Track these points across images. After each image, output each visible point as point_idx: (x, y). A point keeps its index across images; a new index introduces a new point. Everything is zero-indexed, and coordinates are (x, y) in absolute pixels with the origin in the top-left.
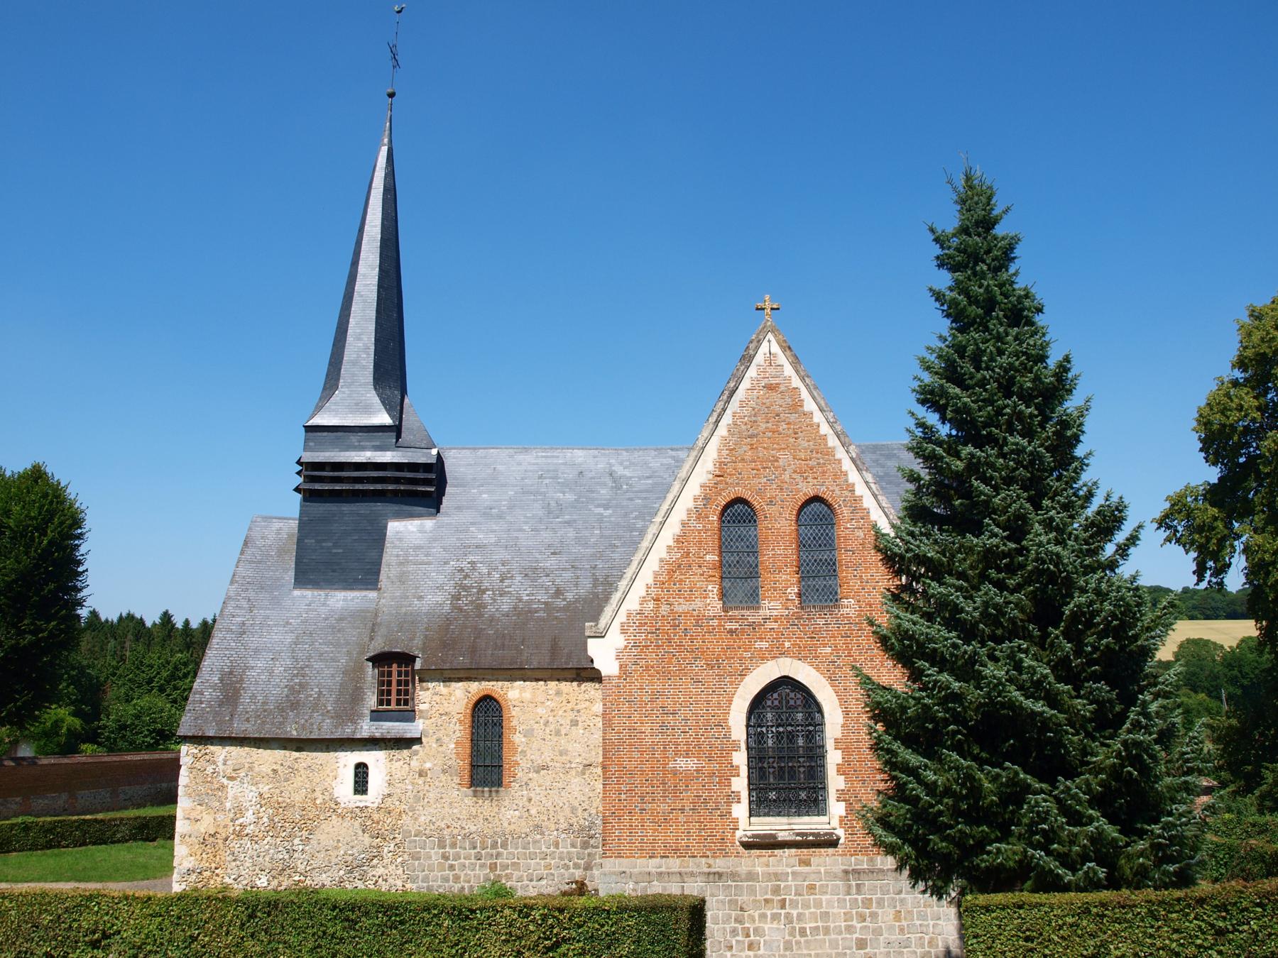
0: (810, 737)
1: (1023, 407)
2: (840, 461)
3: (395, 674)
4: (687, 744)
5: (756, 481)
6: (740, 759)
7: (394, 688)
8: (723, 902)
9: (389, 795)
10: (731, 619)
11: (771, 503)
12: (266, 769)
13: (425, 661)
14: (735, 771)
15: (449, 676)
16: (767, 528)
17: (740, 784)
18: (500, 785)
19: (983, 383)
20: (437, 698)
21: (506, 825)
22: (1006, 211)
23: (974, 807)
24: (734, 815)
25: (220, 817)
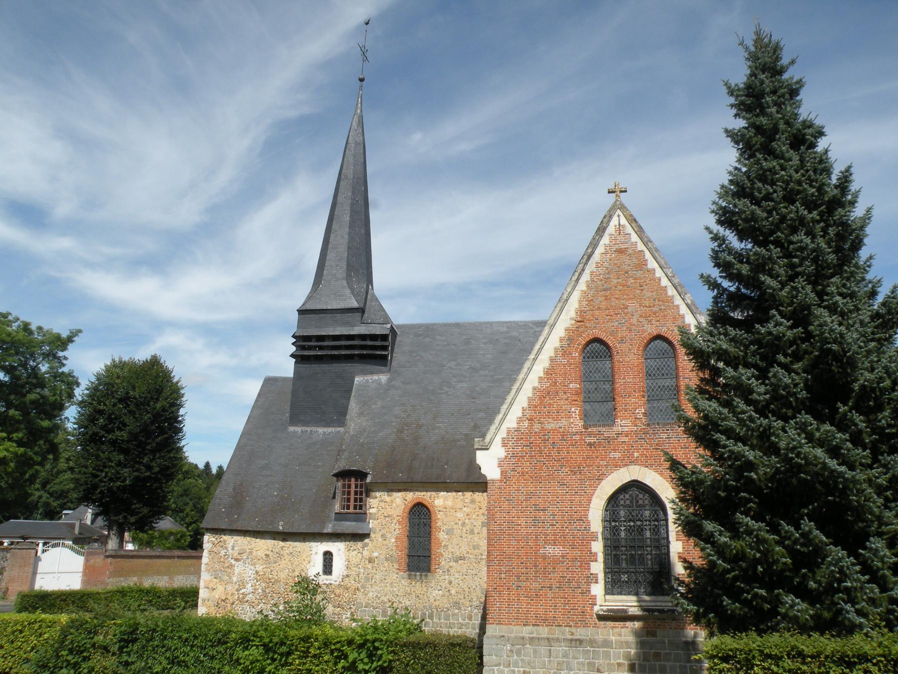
0: (656, 530)
1: (806, 212)
2: (678, 307)
3: (353, 486)
4: (555, 535)
5: (610, 324)
6: (598, 547)
7: (352, 497)
8: (583, 664)
9: (347, 576)
10: (590, 435)
11: (622, 341)
12: (261, 554)
13: (374, 476)
14: (593, 557)
15: (392, 487)
16: (619, 362)
17: (598, 568)
18: (429, 570)
19: (768, 197)
20: (382, 504)
21: (432, 600)
22: (793, 62)
23: (768, 570)
24: (593, 592)
25: (229, 587)
